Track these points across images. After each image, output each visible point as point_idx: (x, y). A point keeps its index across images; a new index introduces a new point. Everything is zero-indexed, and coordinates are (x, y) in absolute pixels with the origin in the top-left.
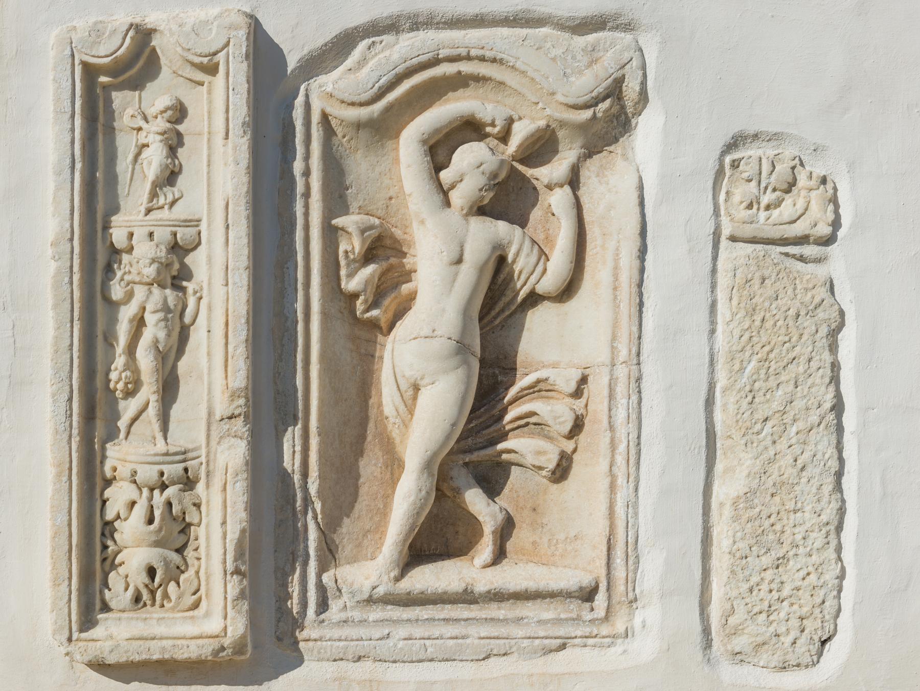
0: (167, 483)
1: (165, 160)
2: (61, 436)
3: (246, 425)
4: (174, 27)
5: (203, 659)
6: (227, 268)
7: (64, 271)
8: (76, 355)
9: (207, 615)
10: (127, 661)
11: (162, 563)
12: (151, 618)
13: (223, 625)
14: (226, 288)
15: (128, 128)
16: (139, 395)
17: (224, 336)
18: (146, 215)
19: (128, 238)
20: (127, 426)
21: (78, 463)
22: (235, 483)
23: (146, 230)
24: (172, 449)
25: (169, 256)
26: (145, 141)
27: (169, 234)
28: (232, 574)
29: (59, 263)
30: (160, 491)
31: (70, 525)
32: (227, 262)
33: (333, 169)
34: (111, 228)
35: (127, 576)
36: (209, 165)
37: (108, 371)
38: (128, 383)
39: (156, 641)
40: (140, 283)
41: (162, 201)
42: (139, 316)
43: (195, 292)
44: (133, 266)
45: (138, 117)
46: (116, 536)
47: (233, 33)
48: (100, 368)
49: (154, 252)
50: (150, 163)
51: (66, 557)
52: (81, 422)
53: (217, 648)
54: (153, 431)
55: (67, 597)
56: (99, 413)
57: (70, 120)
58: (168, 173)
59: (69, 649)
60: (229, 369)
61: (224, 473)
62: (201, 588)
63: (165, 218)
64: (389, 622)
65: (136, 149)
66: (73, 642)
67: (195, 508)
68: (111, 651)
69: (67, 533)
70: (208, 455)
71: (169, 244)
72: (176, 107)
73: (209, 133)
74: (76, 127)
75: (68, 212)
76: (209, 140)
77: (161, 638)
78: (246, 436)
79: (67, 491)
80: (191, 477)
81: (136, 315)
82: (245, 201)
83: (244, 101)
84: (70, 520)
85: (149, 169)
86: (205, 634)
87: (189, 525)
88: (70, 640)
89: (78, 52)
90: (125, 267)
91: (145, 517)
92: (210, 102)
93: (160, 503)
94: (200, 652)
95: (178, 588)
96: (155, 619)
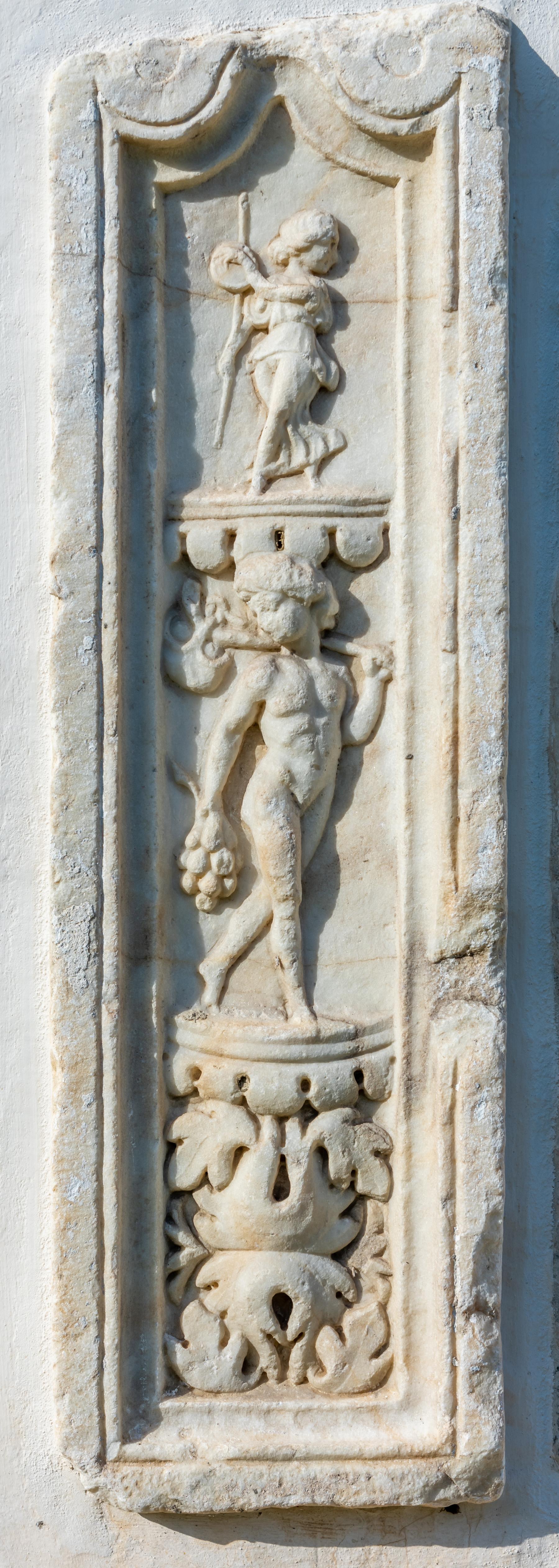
0: (316, 1104)
1: (310, 361)
2: (78, 999)
3: (496, 972)
4: (331, 51)
5: (402, 1504)
6: (455, 610)
7: (81, 621)
8: (109, 814)
9: (409, 1403)
10: (230, 1509)
11: (306, 1287)
12: (281, 1410)
13: (446, 1430)
14: (452, 658)
15: (219, 291)
16: (248, 903)
17: (449, 767)
18: (264, 490)
19: (223, 541)
20: (221, 975)
21: (116, 1061)
22: (474, 1107)
23: (267, 525)
24: (329, 1028)
25: (319, 584)
26: (260, 320)
27: (319, 533)
28: (468, 1313)
29: (71, 604)
30: (300, 1122)
31: (99, 1201)
32: (456, 597)
34: (181, 520)
35: (223, 1314)
36: (408, 373)
37: (179, 847)
38: (224, 877)
39: (296, 1463)
40: (249, 647)
41: (299, 457)
42: (249, 723)
43: (377, 668)
44: (233, 610)
45: (244, 262)
46: (199, 1223)
47: (469, 61)
48: (159, 842)
49: (285, 577)
50: (271, 371)
51: (92, 1275)
52: (120, 967)
53: (434, 1481)
54: (280, 986)
55: (94, 1365)
56: (157, 947)
57: (94, 273)
58: (314, 390)
59: (101, 1480)
60: (461, 844)
61: (450, 1084)
62: (393, 1341)
63: (308, 498)
65: (240, 338)
66: (109, 1466)
67: (377, 1162)
68: (195, 1487)
69: (93, 1220)
70: (408, 1042)
71: (318, 557)
72: (333, 238)
73: (410, 298)
74: (106, 288)
75: (90, 485)
76: (409, 313)
77: (307, 1458)
78: (496, 997)
79: (93, 1124)
80: (370, 1091)
81: (245, 719)
82: (498, 454)
83: (495, 221)
84: (100, 1190)
85: (270, 383)
86: (406, 1450)
87: (362, 1198)
88: (101, 1459)
89: (110, 113)
90: (214, 611)
91: (269, 1184)
92: (411, 226)
93: (301, 1150)
94: (396, 1491)
95: (339, 1343)
96: (289, 1411)
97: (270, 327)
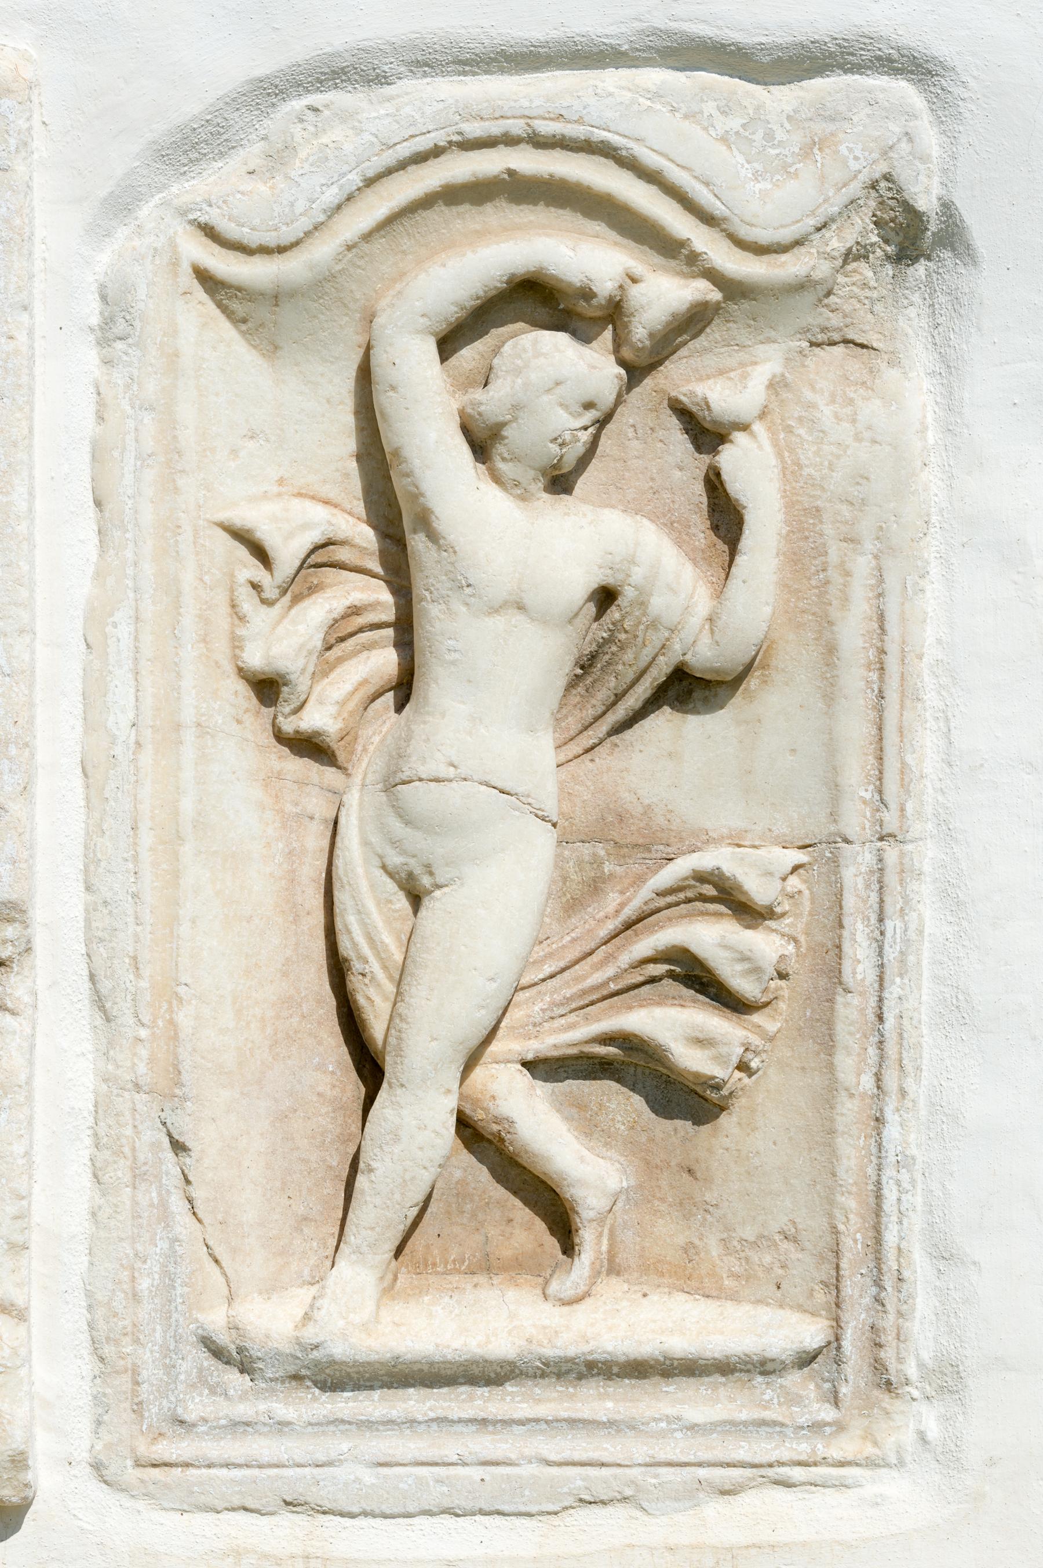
33: (217, 395)
64: (347, 1426)
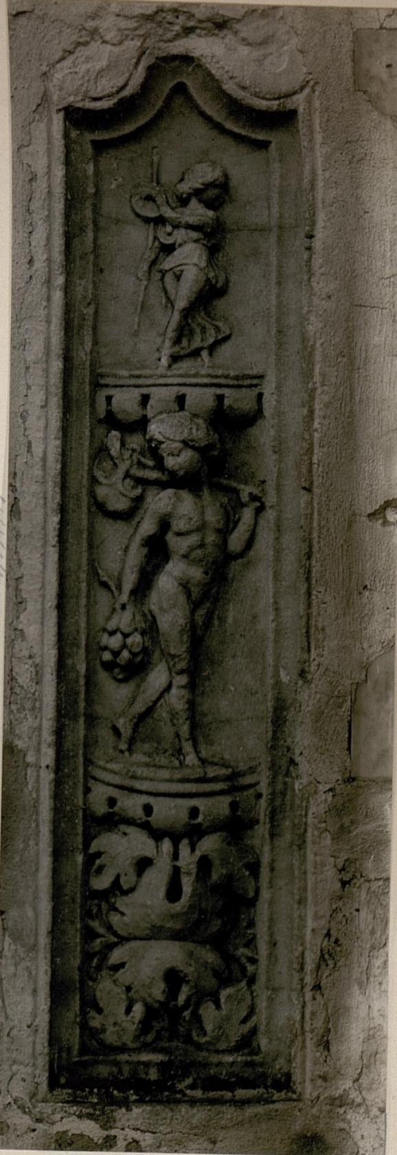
97: (176, 246)
